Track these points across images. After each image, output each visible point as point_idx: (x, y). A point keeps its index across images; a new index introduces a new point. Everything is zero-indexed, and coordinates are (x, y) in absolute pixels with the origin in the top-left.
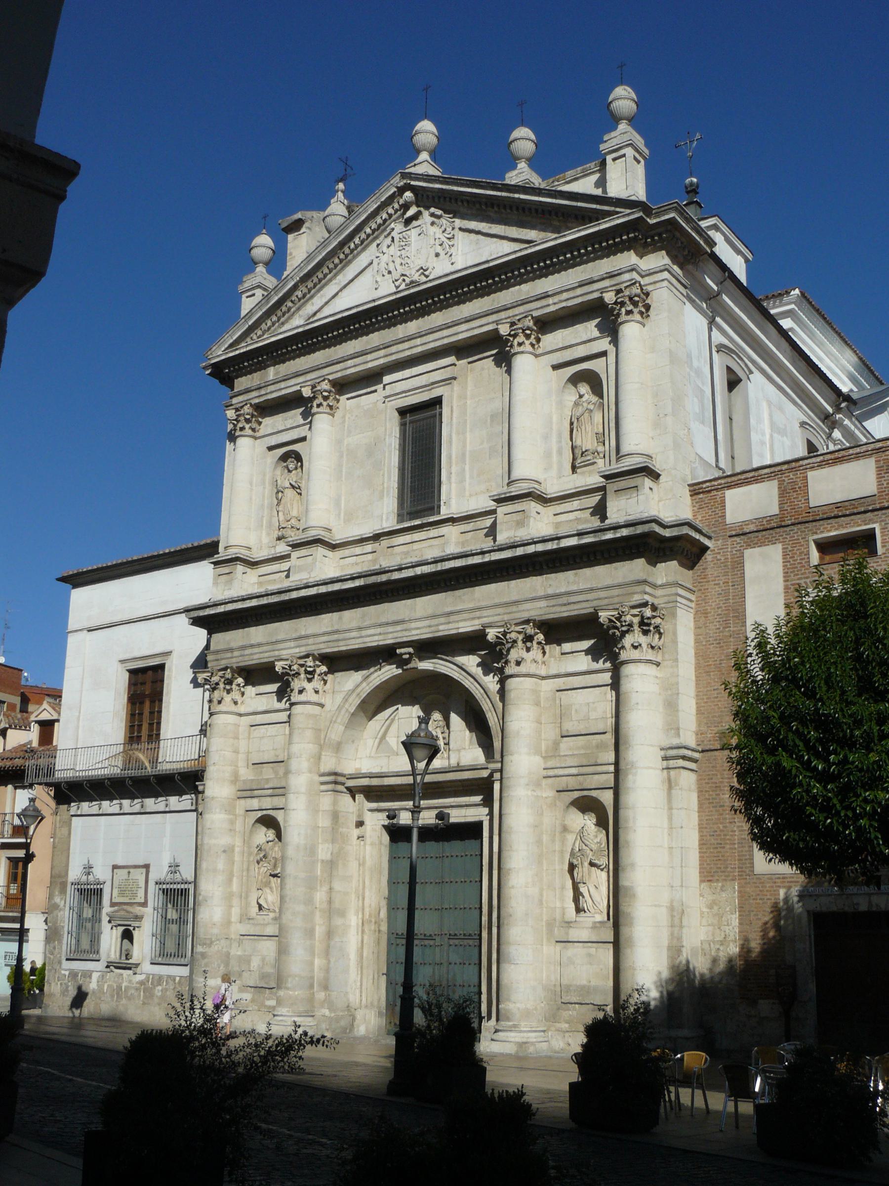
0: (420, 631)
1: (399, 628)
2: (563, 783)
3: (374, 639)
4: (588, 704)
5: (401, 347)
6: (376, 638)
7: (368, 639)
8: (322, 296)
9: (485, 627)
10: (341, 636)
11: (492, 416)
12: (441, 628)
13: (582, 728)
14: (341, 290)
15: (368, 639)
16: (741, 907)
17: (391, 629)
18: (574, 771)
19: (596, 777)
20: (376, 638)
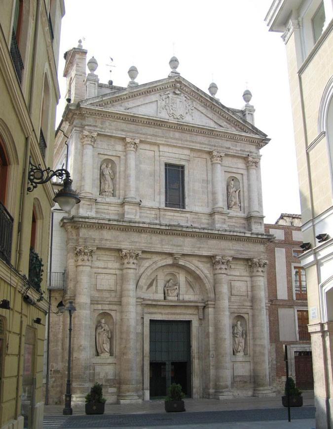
0: (187, 250)
1: (179, 248)
2: (232, 310)
3: (167, 249)
4: (240, 286)
5: (173, 141)
6: (168, 250)
7: (165, 249)
8: (133, 103)
9: (216, 256)
10: (153, 246)
11: (203, 180)
12: (196, 252)
13: (238, 293)
14: (141, 105)
15: (165, 249)
16: (276, 350)
17: (175, 248)
18: (236, 307)
19: (243, 310)
20: (168, 250)
